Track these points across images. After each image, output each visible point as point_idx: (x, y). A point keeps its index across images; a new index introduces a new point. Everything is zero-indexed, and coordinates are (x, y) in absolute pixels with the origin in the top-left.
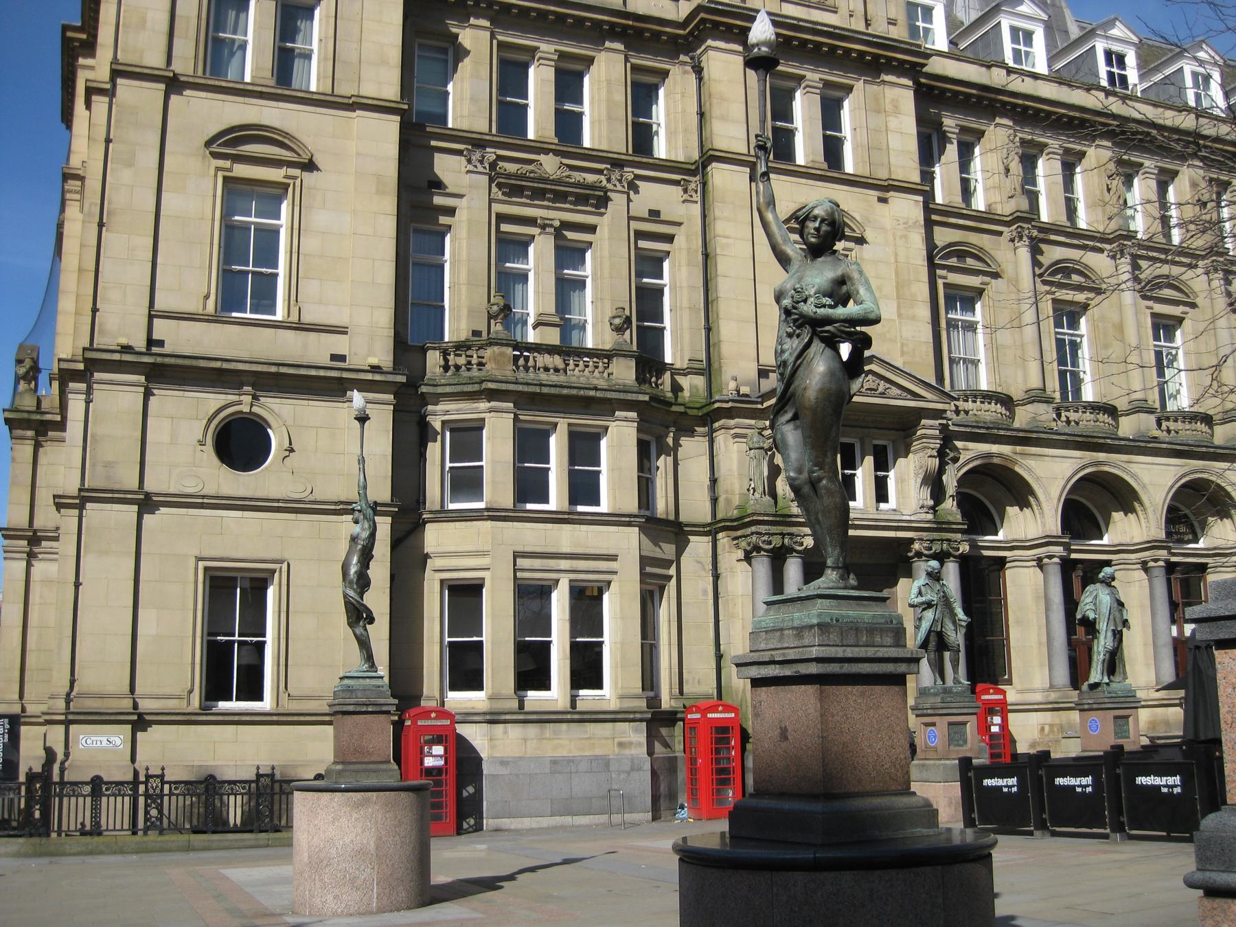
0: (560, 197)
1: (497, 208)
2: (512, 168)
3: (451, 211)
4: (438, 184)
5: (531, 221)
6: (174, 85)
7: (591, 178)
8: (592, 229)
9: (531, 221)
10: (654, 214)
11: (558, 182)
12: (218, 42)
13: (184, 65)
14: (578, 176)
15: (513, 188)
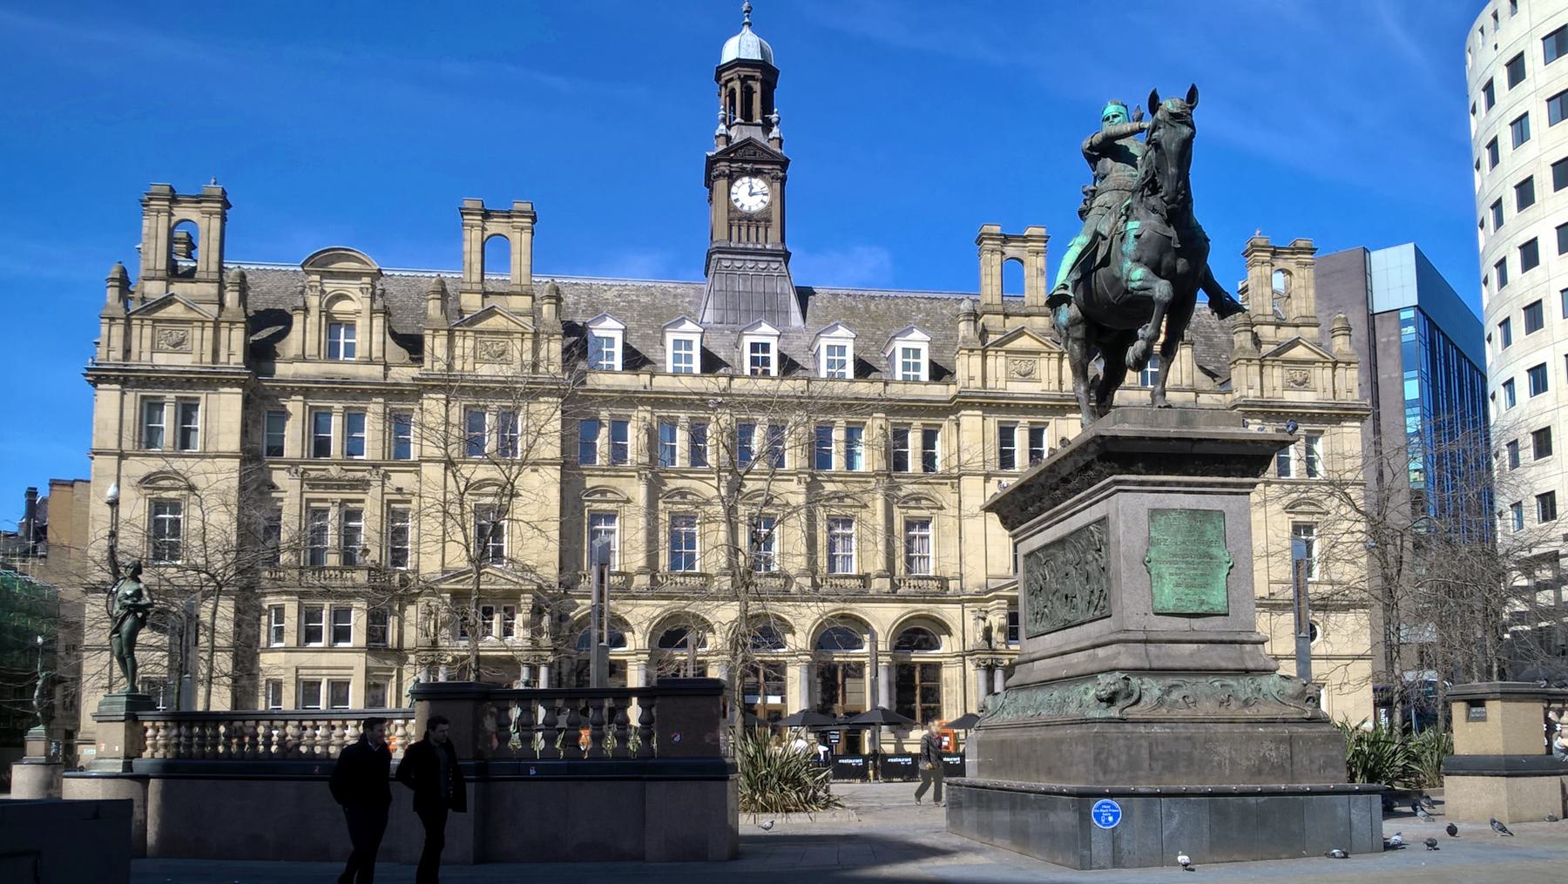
0: (340, 487)
1: (306, 496)
2: (313, 474)
3: (281, 499)
4: (273, 487)
5: (325, 500)
6: (122, 456)
7: (359, 475)
8: (362, 501)
9: (325, 500)
10: (399, 490)
11: (340, 479)
12: (150, 429)
13: (127, 446)
14: (350, 475)
15: (314, 485)
